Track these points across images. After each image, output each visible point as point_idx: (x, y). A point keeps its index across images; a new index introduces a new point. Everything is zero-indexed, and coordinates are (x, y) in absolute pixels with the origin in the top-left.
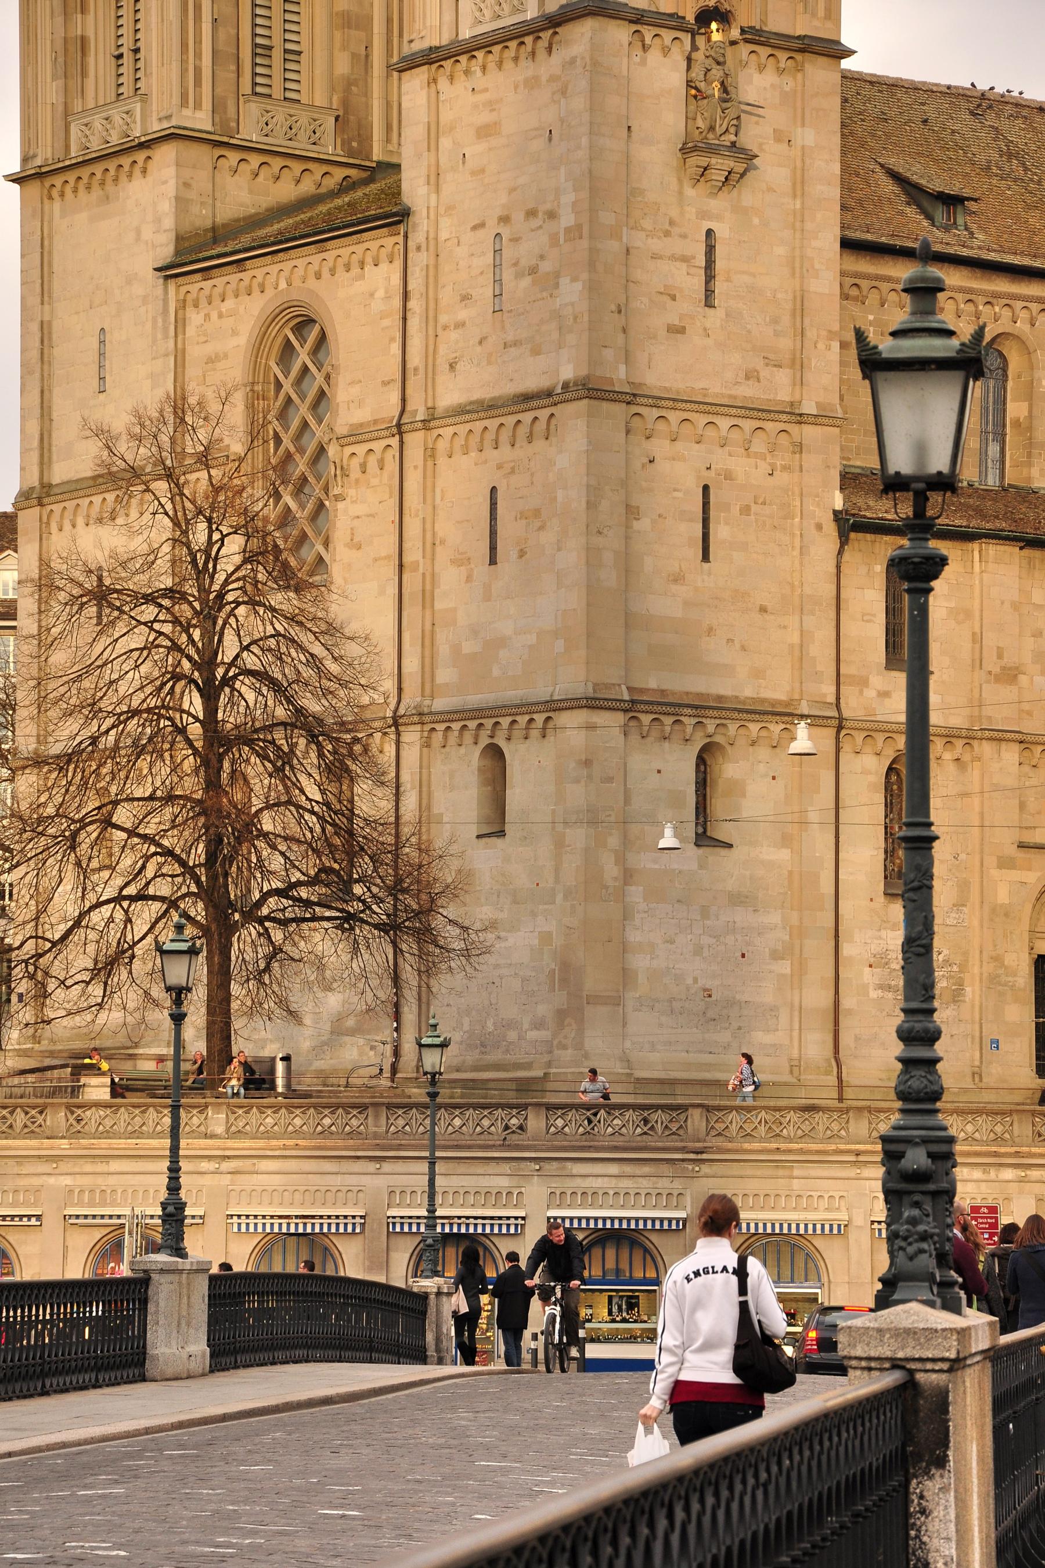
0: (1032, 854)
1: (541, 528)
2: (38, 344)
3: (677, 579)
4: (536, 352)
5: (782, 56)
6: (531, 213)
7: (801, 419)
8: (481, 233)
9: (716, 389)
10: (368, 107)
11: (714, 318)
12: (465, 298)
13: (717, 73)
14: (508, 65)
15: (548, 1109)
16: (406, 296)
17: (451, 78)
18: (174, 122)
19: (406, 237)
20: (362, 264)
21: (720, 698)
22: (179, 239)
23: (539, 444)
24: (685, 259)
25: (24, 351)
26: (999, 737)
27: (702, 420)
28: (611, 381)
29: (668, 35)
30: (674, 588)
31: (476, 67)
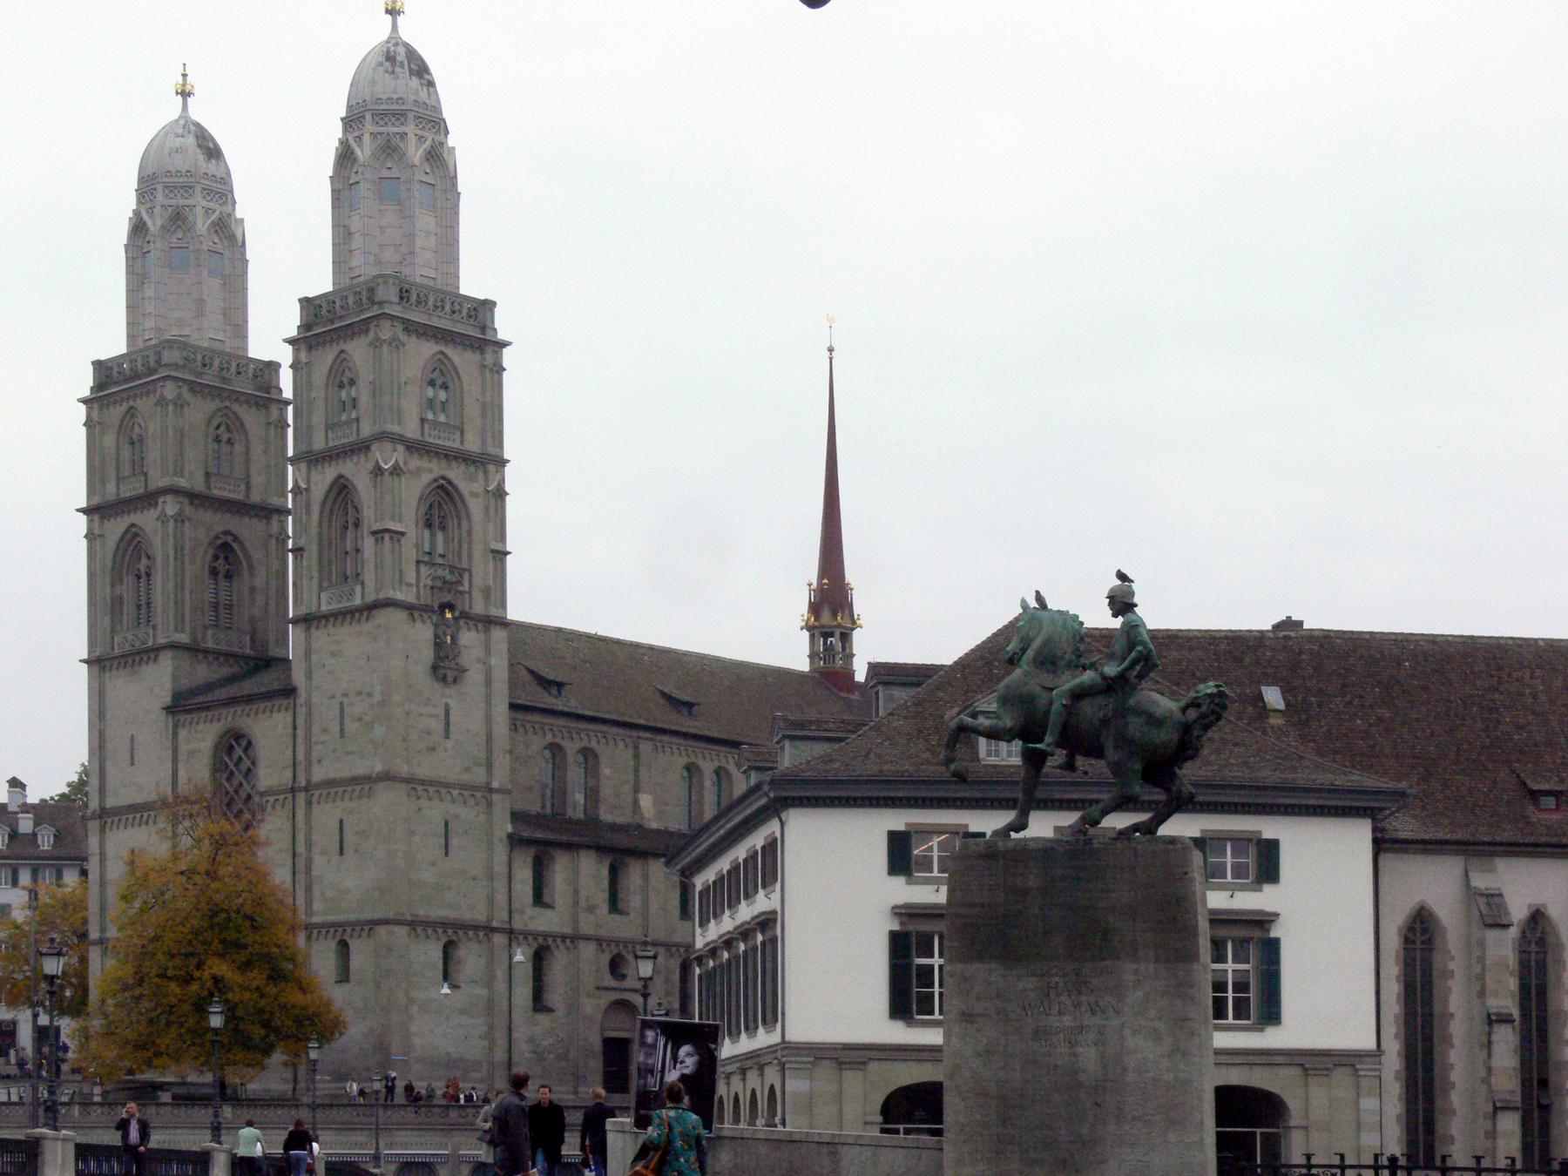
4: (362, 757)
6: (359, 693)
7: (491, 790)
9: (452, 777)
11: (449, 744)
13: (449, 631)
16: (295, 728)
26: (587, 938)
31: (330, 625)
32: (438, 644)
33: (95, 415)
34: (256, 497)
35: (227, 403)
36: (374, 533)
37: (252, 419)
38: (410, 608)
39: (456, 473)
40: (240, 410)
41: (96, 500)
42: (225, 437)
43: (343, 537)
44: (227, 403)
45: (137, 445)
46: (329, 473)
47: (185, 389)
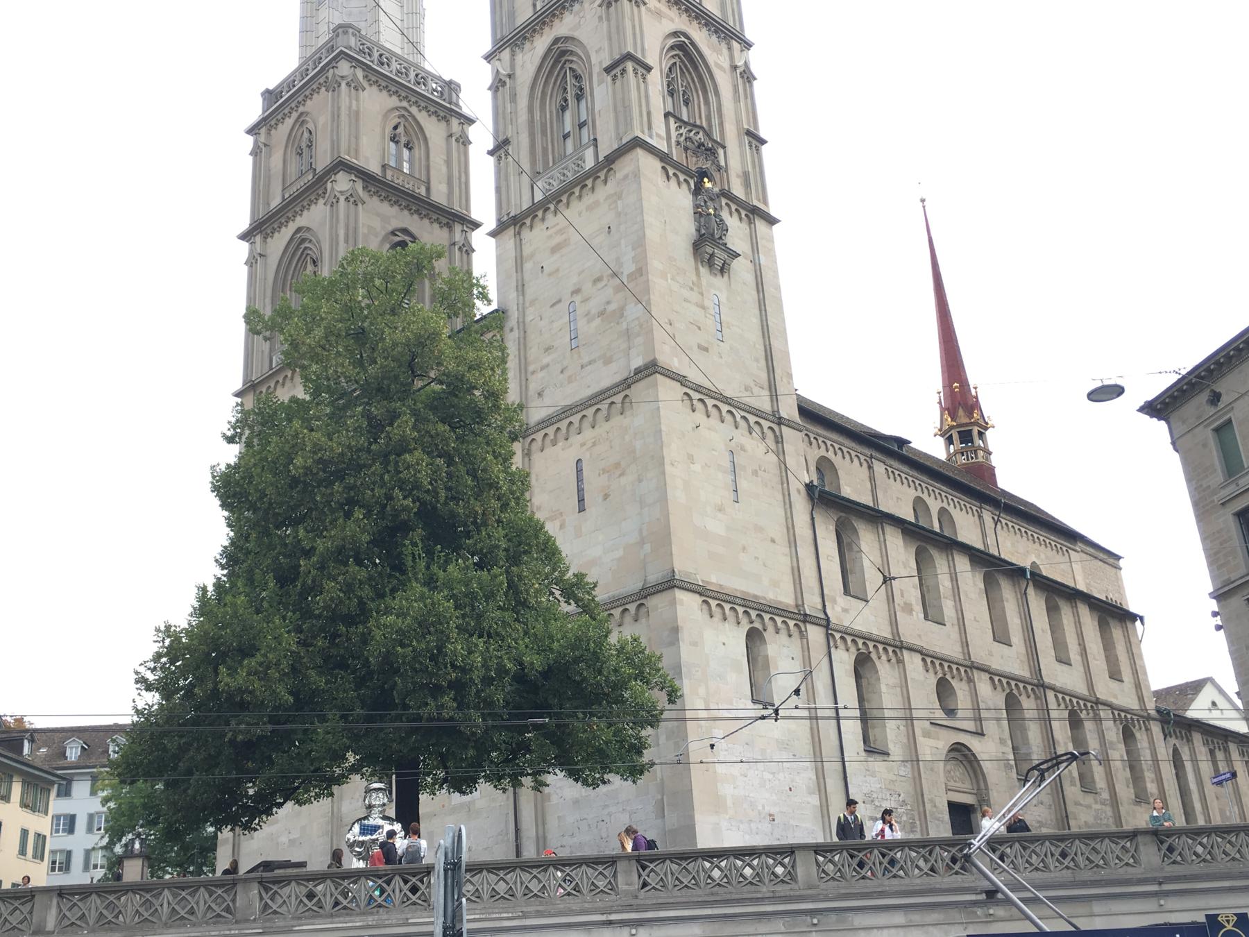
0: (937, 729)
1: (622, 475)
3: (720, 509)
4: (608, 361)
5: (743, 213)
6: (599, 279)
7: (780, 421)
14: (575, 204)
15: (816, 853)
21: (755, 596)
23: (617, 420)
26: (911, 649)
27: (724, 408)
29: (682, 177)
30: (719, 515)
31: (550, 216)
32: (699, 215)
33: (262, 138)
35: (405, 104)
36: (608, 70)
37: (434, 129)
38: (664, 158)
39: (700, 36)
40: (422, 117)
42: (403, 140)
43: (561, 120)
44: (405, 104)
45: (305, 150)
46: (541, 43)
47: (360, 74)
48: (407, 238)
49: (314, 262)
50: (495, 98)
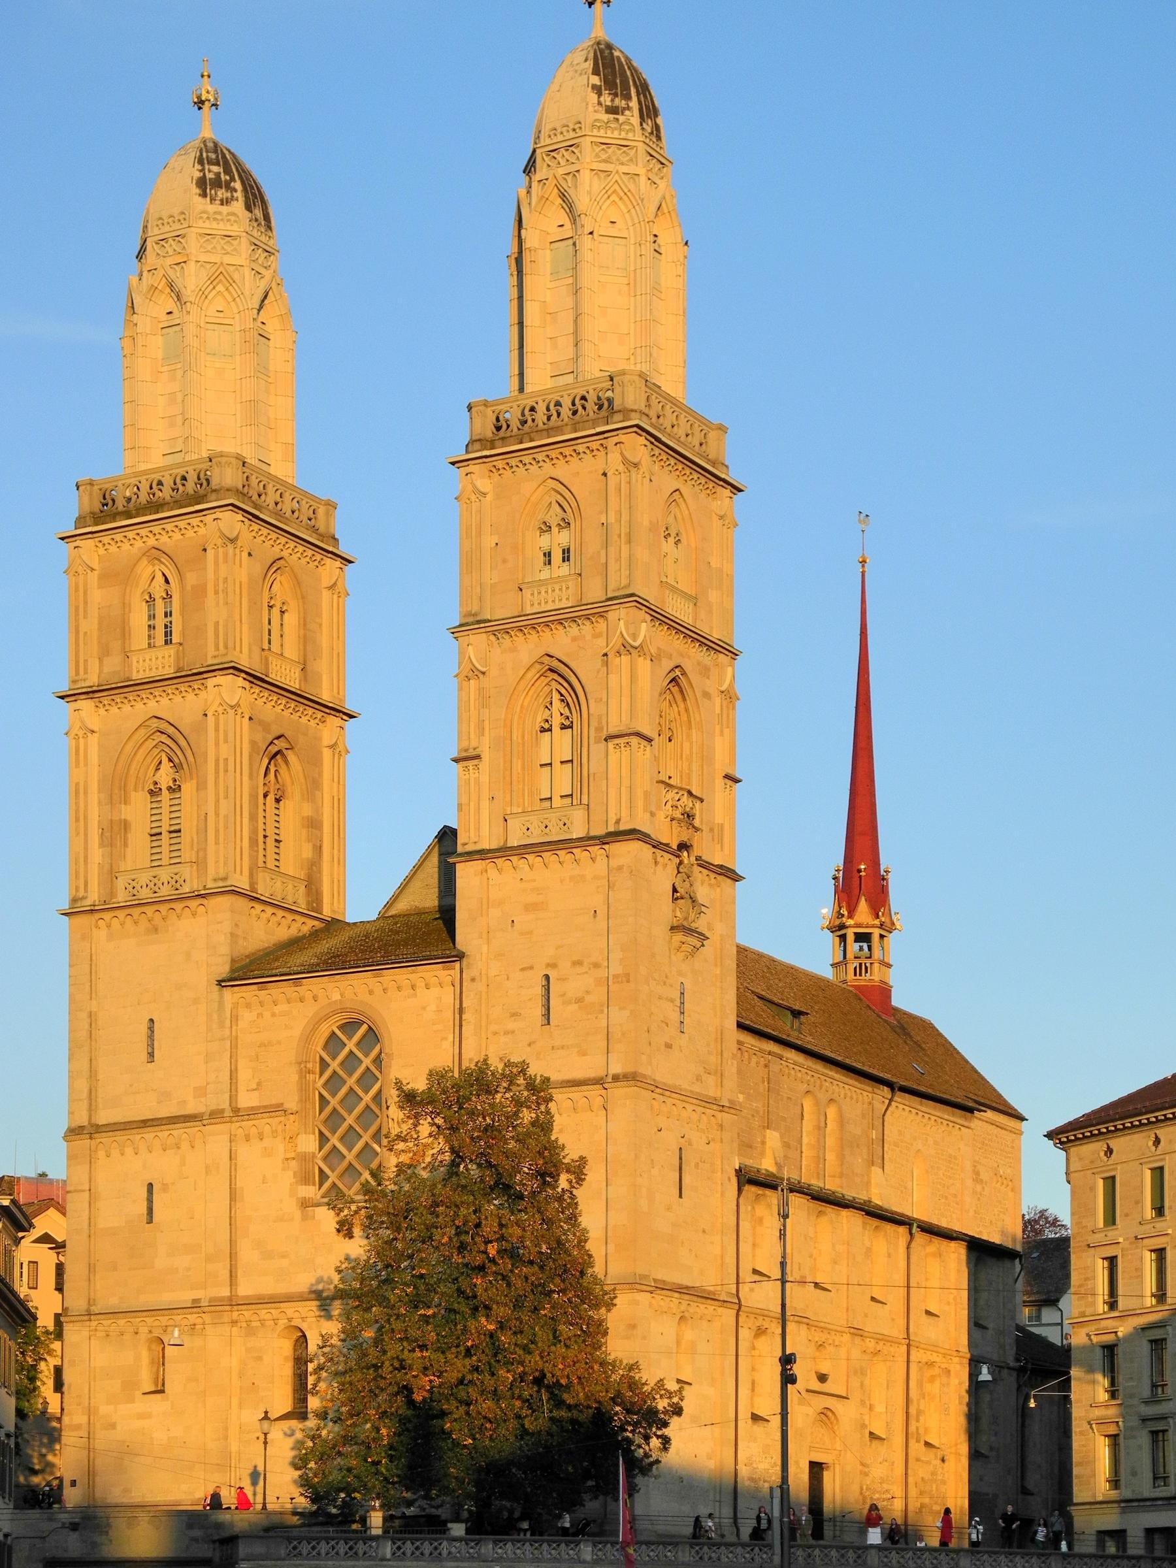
2: (87, 1026)
3: (669, 1209)
4: (583, 1053)
5: (712, 875)
6: (577, 963)
8: (528, 973)
9: (685, 1085)
10: (321, 881)
12: (514, 1015)
17: (500, 871)
18: (229, 883)
19: (461, 972)
20: (413, 987)
22: (233, 961)
24: (672, 1001)
25: (72, 1031)
28: (644, 1076)
34: (310, 692)
38: (657, 845)
41: (93, 680)
48: (281, 744)
49: (170, 760)
50: (460, 689)
